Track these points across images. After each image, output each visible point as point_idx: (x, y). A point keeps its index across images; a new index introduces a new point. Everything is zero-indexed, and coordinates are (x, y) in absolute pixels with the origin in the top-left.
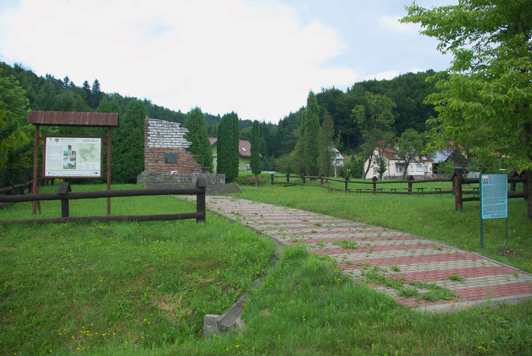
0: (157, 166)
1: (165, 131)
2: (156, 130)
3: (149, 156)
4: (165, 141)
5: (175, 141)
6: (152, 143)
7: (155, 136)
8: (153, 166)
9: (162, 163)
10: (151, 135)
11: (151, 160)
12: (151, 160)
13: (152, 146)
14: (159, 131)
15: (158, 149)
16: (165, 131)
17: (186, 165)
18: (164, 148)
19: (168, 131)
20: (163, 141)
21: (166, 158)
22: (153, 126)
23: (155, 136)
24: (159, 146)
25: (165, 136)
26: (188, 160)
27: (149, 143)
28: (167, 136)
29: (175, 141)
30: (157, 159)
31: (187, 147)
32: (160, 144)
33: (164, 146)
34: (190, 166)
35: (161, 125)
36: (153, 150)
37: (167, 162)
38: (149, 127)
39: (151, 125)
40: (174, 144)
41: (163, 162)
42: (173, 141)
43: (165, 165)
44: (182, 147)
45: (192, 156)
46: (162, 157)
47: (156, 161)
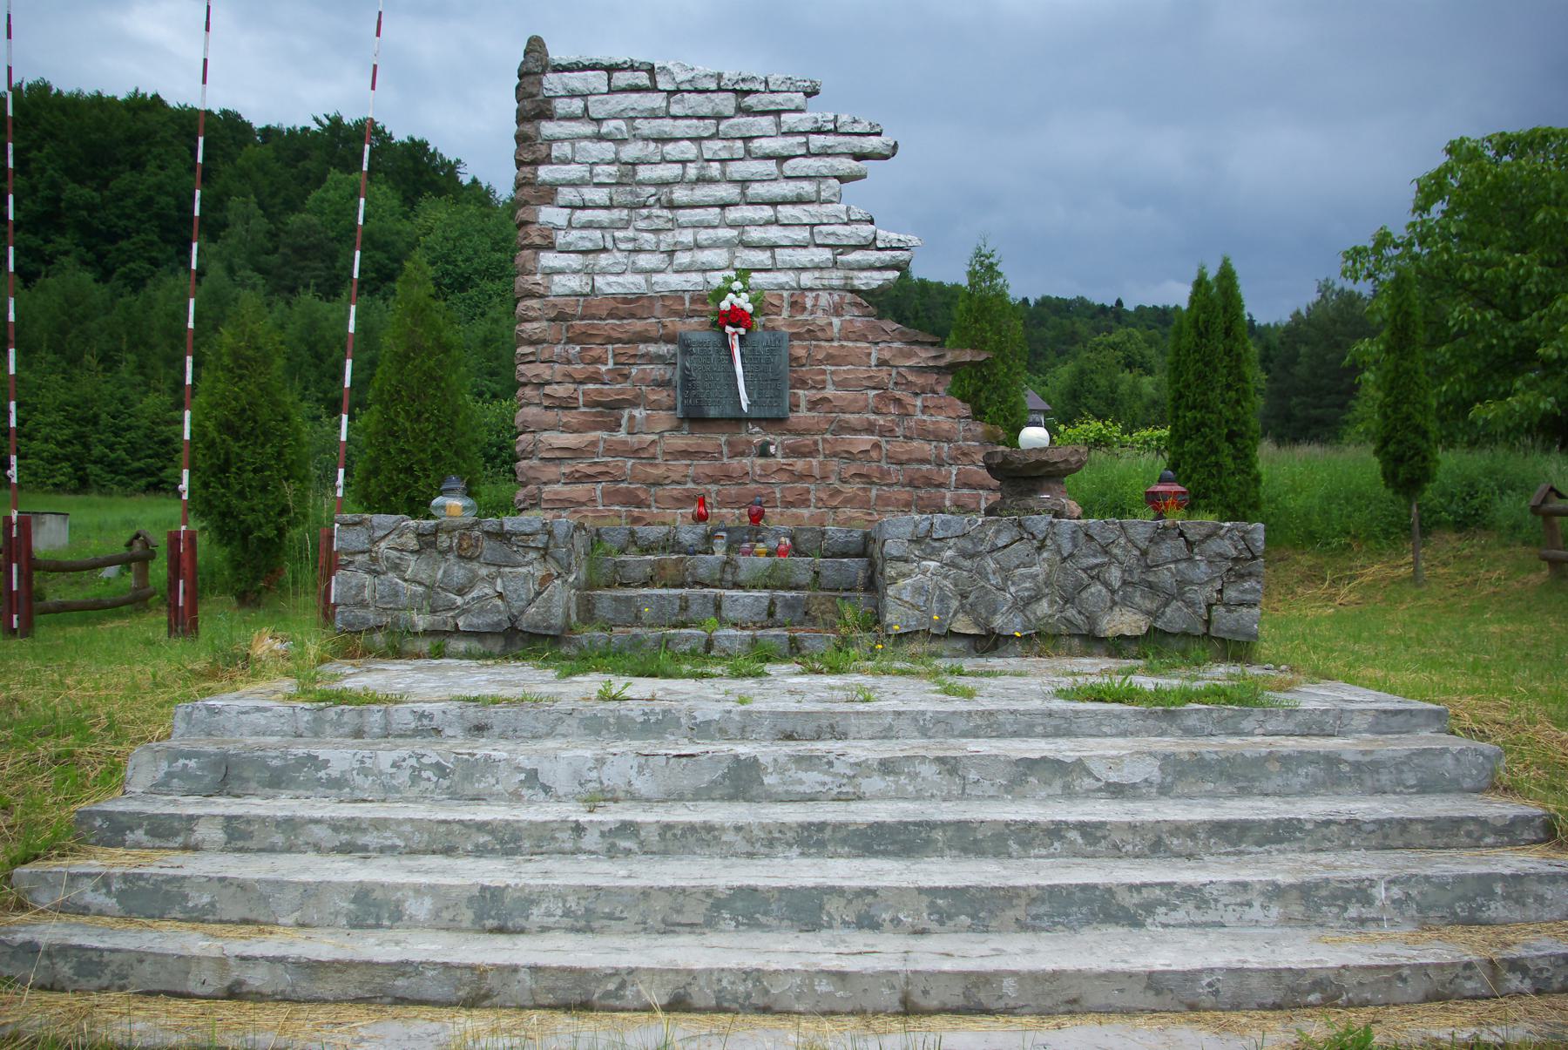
0: (611, 450)
1: (689, 149)
2: (608, 150)
3: (545, 372)
4: (686, 236)
5: (774, 234)
6: (575, 261)
7: (600, 195)
8: (576, 453)
9: (651, 425)
10: (567, 195)
11: (566, 405)
12: (566, 405)
13: (575, 283)
14: (630, 151)
15: (630, 305)
16: (689, 149)
17: (864, 441)
18: (677, 295)
19: (713, 148)
20: (667, 239)
21: (687, 381)
22: (585, 115)
23: (600, 195)
24: (632, 283)
25: (680, 195)
26: (886, 397)
27: (548, 259)
28: (701, 193)
29: (774, 234)
30: (613, 390)
31: (875, 279)
32: (644, 261)
33: (674, 281)
34: (898, 447)
35: (657, 101)
36: (581, 320)
37: (694, 418)
38: (548, 128)
39: (561, 106)
40: (763, 257)
41: (664, 419)
42: (755, 234)
43: (680, 441)
44: (835, 278)
45: (923, 356)
46: (657, 371)
47: (608, 412)
